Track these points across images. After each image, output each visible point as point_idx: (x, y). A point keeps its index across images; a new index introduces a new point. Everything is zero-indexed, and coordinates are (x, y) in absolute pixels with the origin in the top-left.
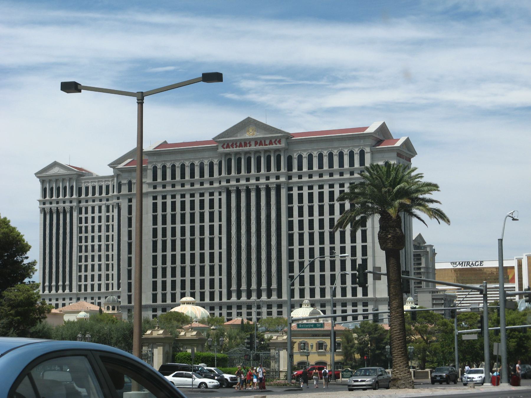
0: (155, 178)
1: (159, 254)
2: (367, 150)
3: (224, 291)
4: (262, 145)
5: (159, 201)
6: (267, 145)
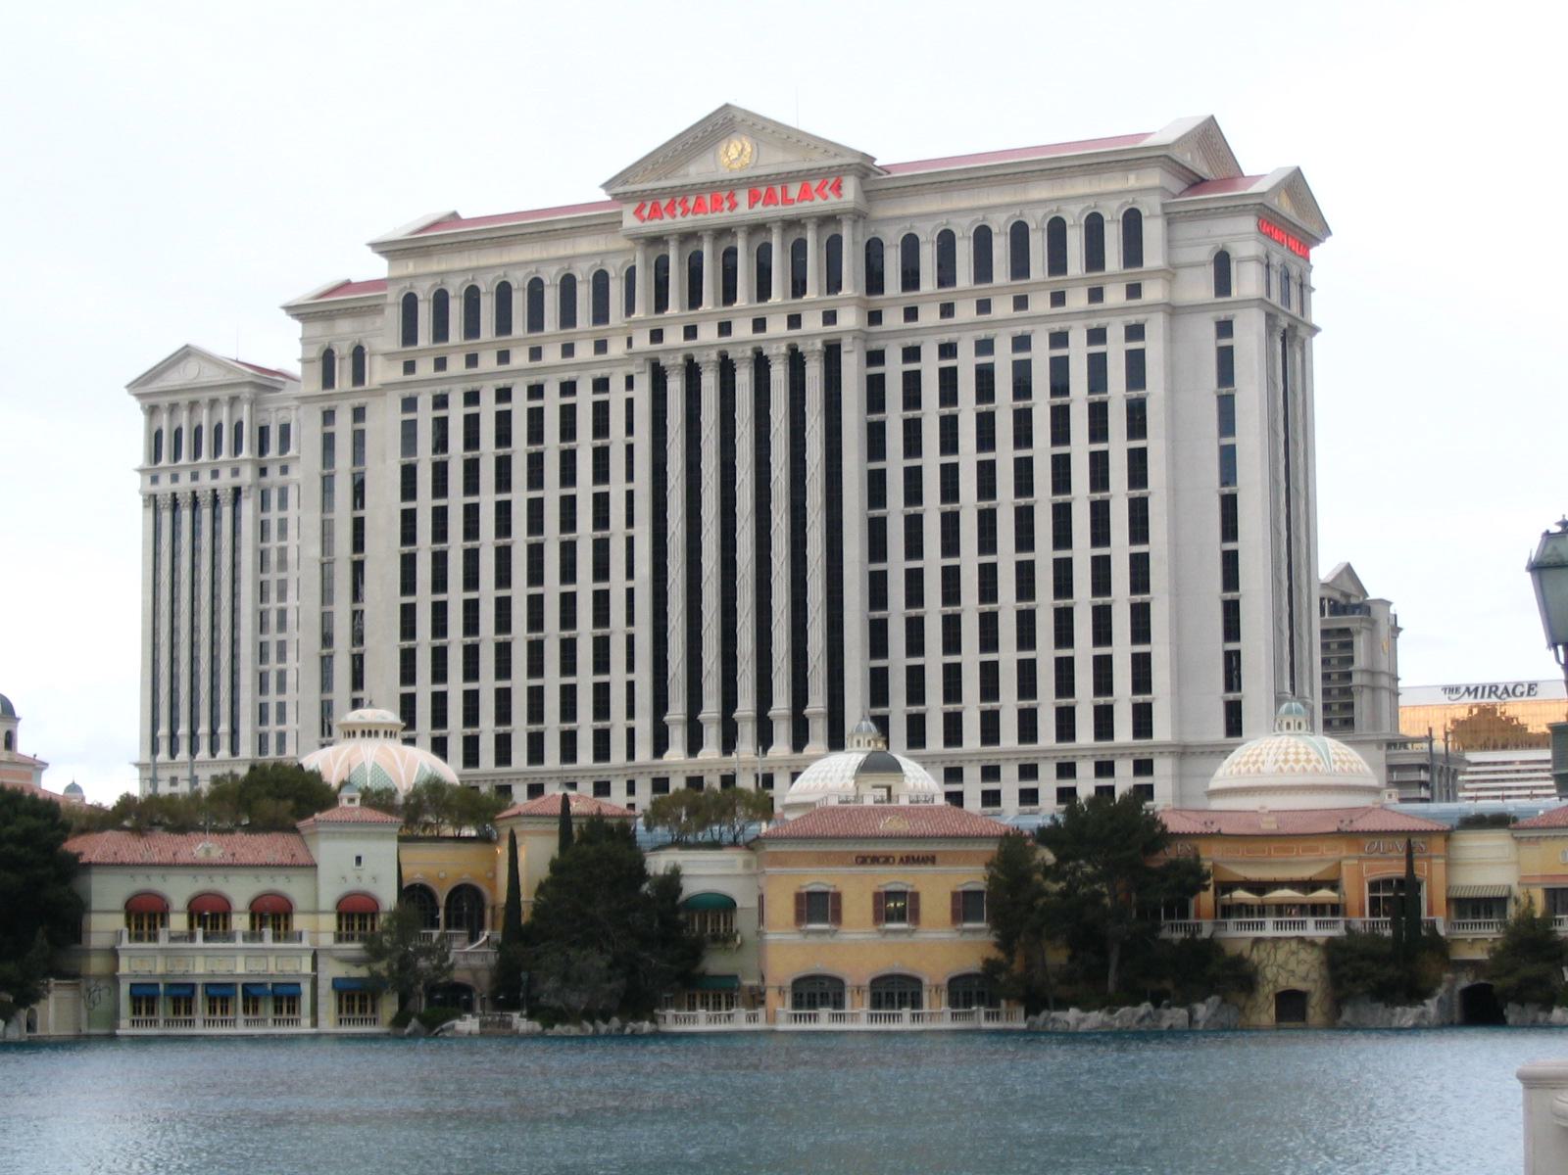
0: (409, 336)
1: (424, 599)
3: (644, 725)
4: (777, 204)
6: (792, 201)
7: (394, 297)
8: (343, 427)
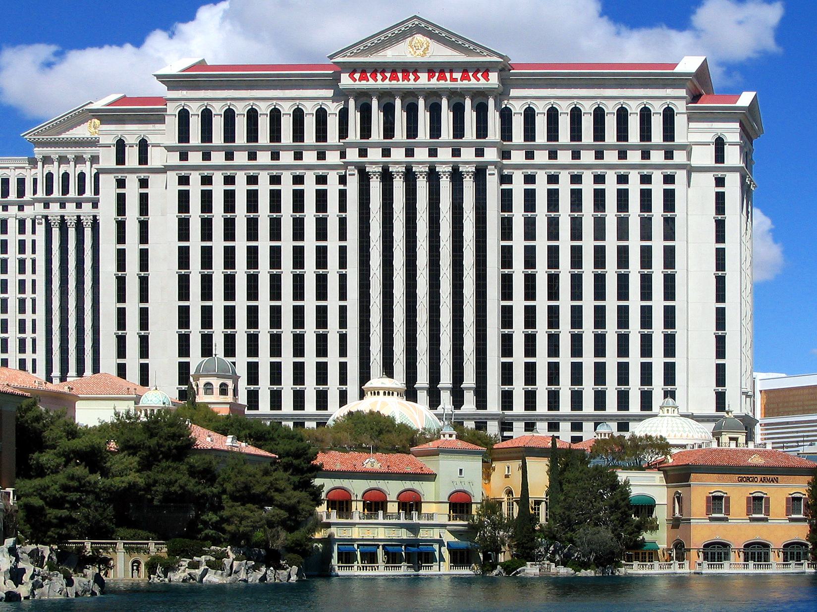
0: (184, 135)
2: (680, 107)
5: (195, 189)
7: (173, 109)
8: (132, 191)
